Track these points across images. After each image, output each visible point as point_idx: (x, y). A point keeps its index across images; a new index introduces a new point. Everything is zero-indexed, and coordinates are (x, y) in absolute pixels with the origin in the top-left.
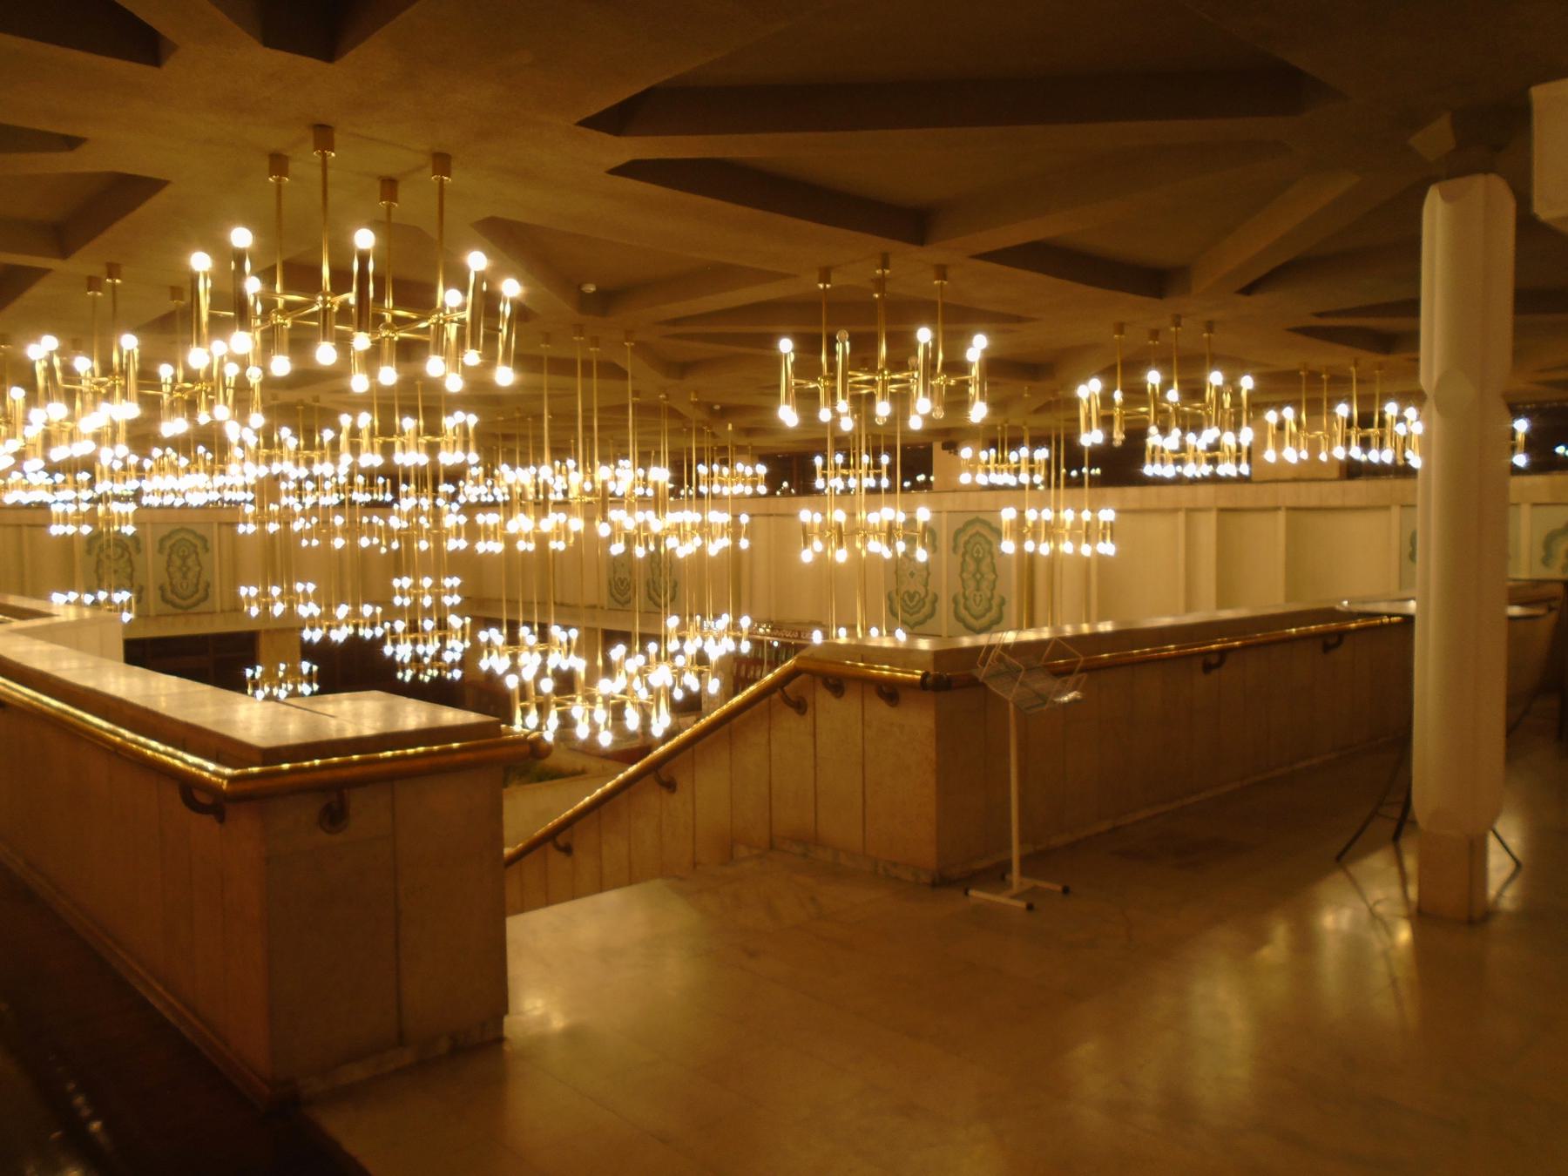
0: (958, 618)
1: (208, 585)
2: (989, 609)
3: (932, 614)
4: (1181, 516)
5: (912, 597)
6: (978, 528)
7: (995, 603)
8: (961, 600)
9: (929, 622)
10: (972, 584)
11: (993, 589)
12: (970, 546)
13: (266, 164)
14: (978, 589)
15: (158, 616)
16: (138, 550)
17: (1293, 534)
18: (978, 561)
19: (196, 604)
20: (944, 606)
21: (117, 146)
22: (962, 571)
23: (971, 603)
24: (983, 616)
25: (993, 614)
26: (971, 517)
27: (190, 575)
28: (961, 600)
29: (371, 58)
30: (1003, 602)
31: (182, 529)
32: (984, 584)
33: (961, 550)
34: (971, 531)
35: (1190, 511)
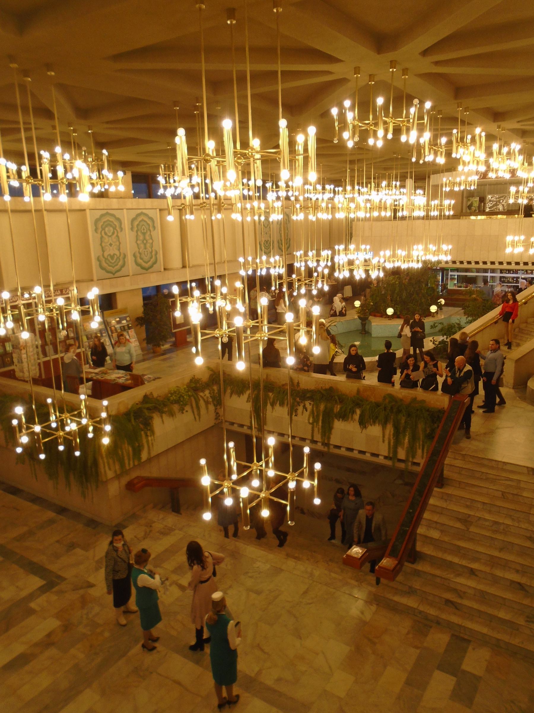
2: (151, 258)
3: (123, 266)
5: (112, 257)
7: (154, 253)
8: (138, 255)
9: (123, 269)
10: (142, 246)
11: (152, 247)
12: (139, 227)
14: (145, 248)
18: (144, 234)
20: (130, 259)
22: (137, 240)
24: (149, 261)
25: (153, 259)
28: (138, 255)
33: (135, 229)
34: (140, 219)
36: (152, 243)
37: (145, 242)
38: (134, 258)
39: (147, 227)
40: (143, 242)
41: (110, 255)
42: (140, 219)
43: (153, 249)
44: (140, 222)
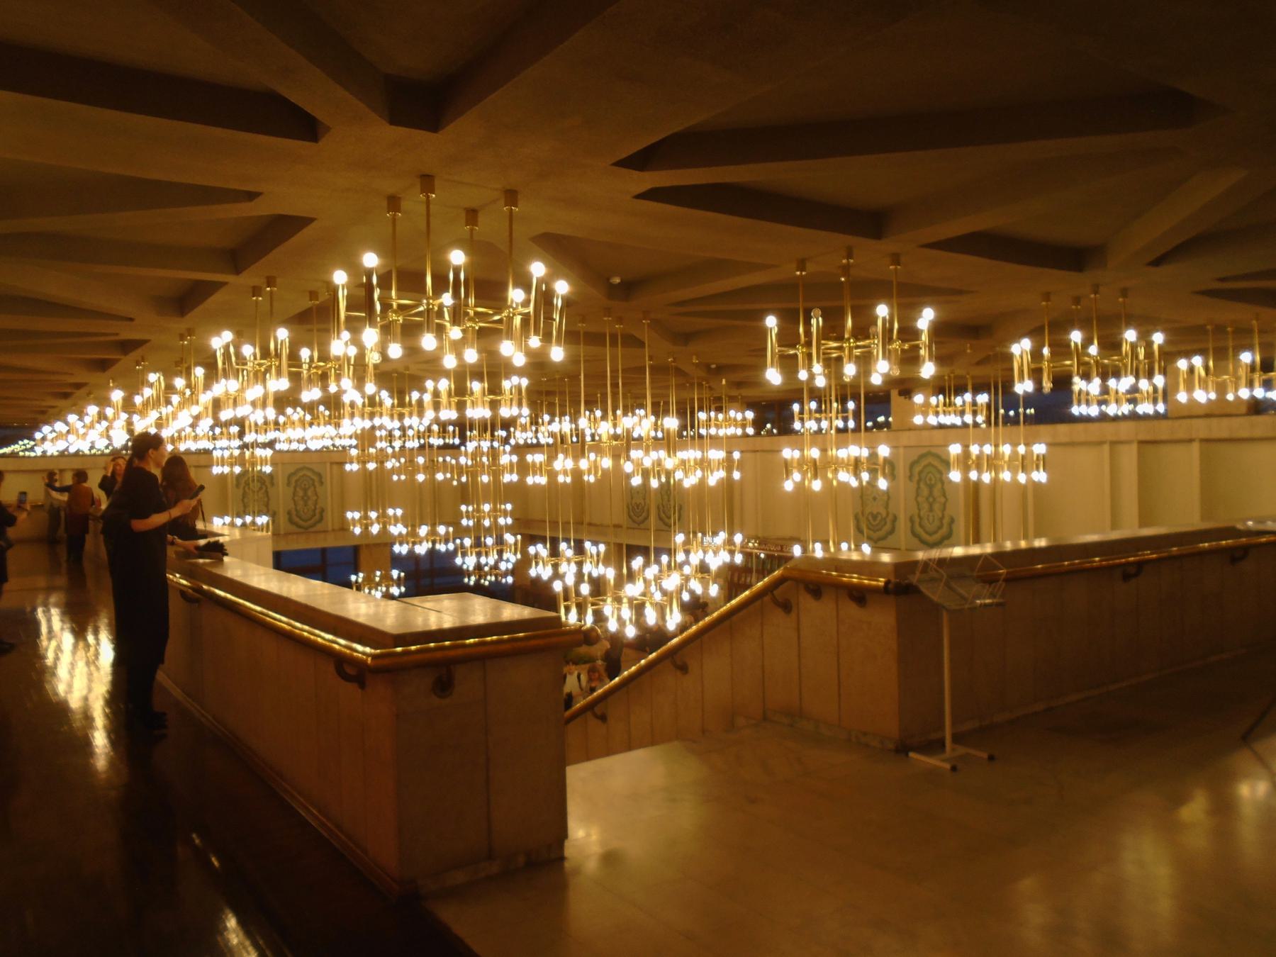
0: (914, 534)
1: (323, 510)
2: (940, 527)
3: (892, 531)
4: (1106, 448)
5: (875, 517)
6: (930, 460)
7: (946, 521)
8: (917, 520)
10: (926, 506)
11: (944, 509)
13: (385, 203)
14: (931, 510)
15: (287, 534)
16: (273, 484)
17: (1206, 461)
18: (931, 487)
19: (314, 525)
21: (281, 197)
22: (918, 495)
23: (925, 522)
24: (936, 532)
25: (945, 530)
26: (924, 451)
27: (310, 503)
28: (917, 520)
29: (464, 129)
30: (952, 521)
31: (302, 469)
32: (936, 507)
33: (916, 478)
35: (1114, 443)
36: (945, 504)
38: (909, 524)
41: (872, 514)
43: (946, 513)
44: (925, 467)
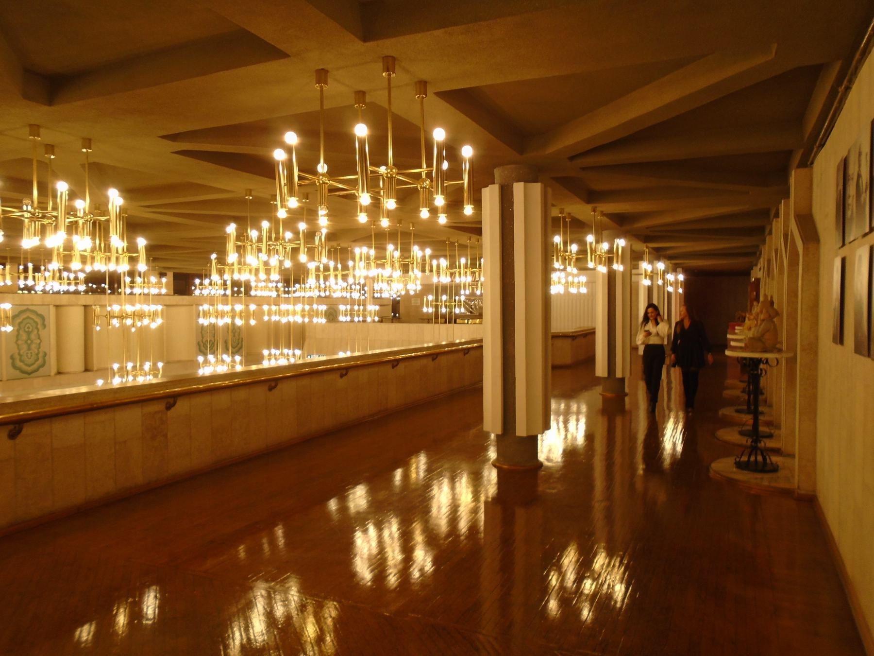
2: (37, 360)
7: (41, 355)
8: (17, 357)
10: (25, 347)
11: (39, 348)
12: (22, 325)
14: (29, 349)
18: (29, 333)
22: (17, 340)
24: (33, 364)
26: (24, 308)
28: (17, 357)
30: (45, 354)
32: (33, 346)
34: (24, 316)
37: (29, 342)
39: (34, 325)
40: (26, 342)
42: (24, 316)
44: (24, 319)
